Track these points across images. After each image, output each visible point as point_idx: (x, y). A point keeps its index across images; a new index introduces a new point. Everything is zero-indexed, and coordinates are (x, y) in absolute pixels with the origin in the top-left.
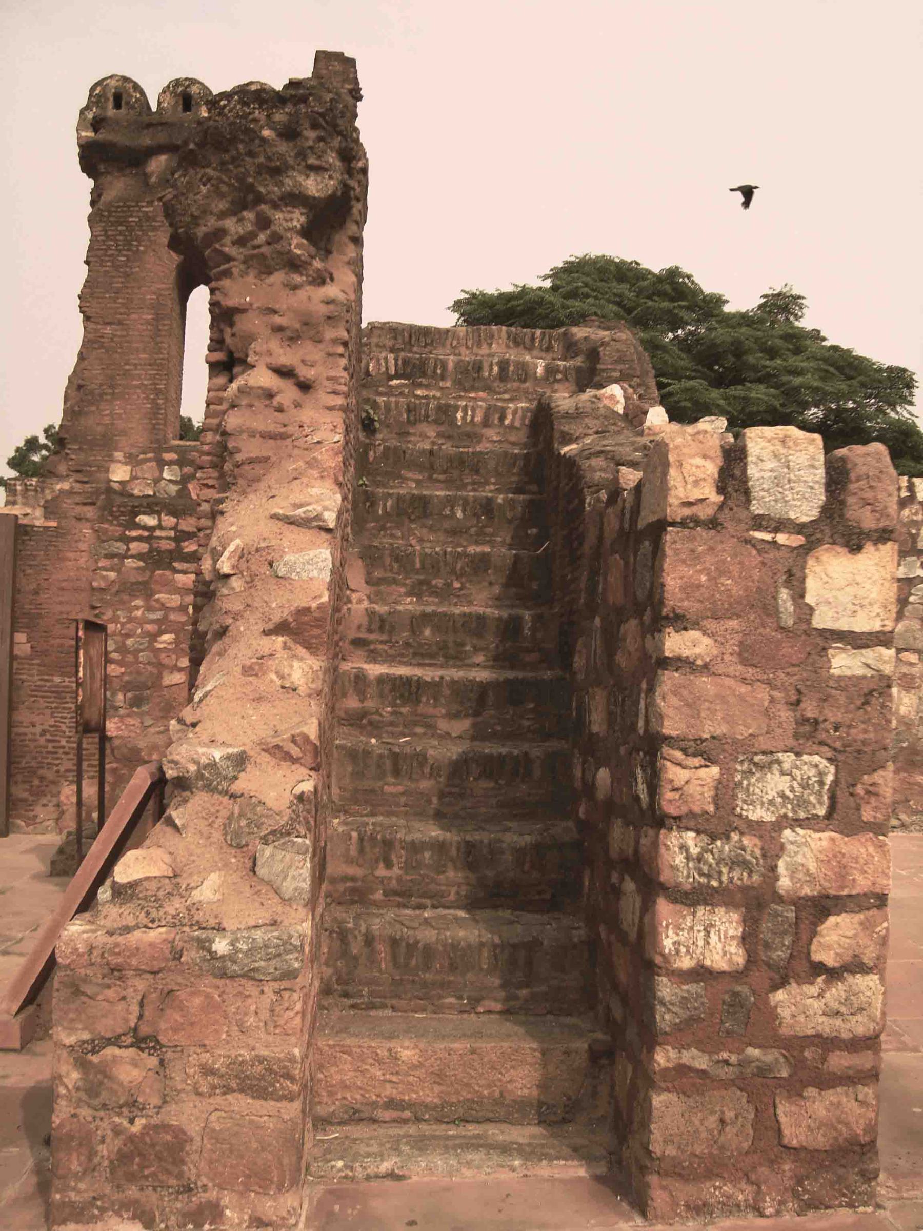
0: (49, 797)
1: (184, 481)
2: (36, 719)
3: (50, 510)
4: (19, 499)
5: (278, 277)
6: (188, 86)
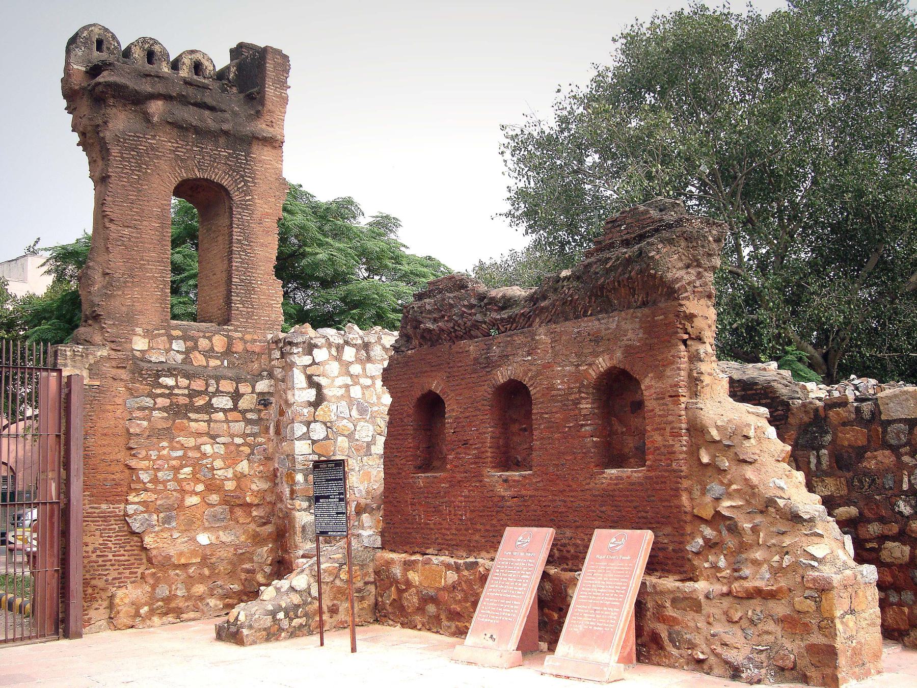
0: (100, 602)
1: (187, 352)
2: (87, 539)
3: (94, 370)
4: (69, 362)
5: (703, 301)
6: (152, 45)
